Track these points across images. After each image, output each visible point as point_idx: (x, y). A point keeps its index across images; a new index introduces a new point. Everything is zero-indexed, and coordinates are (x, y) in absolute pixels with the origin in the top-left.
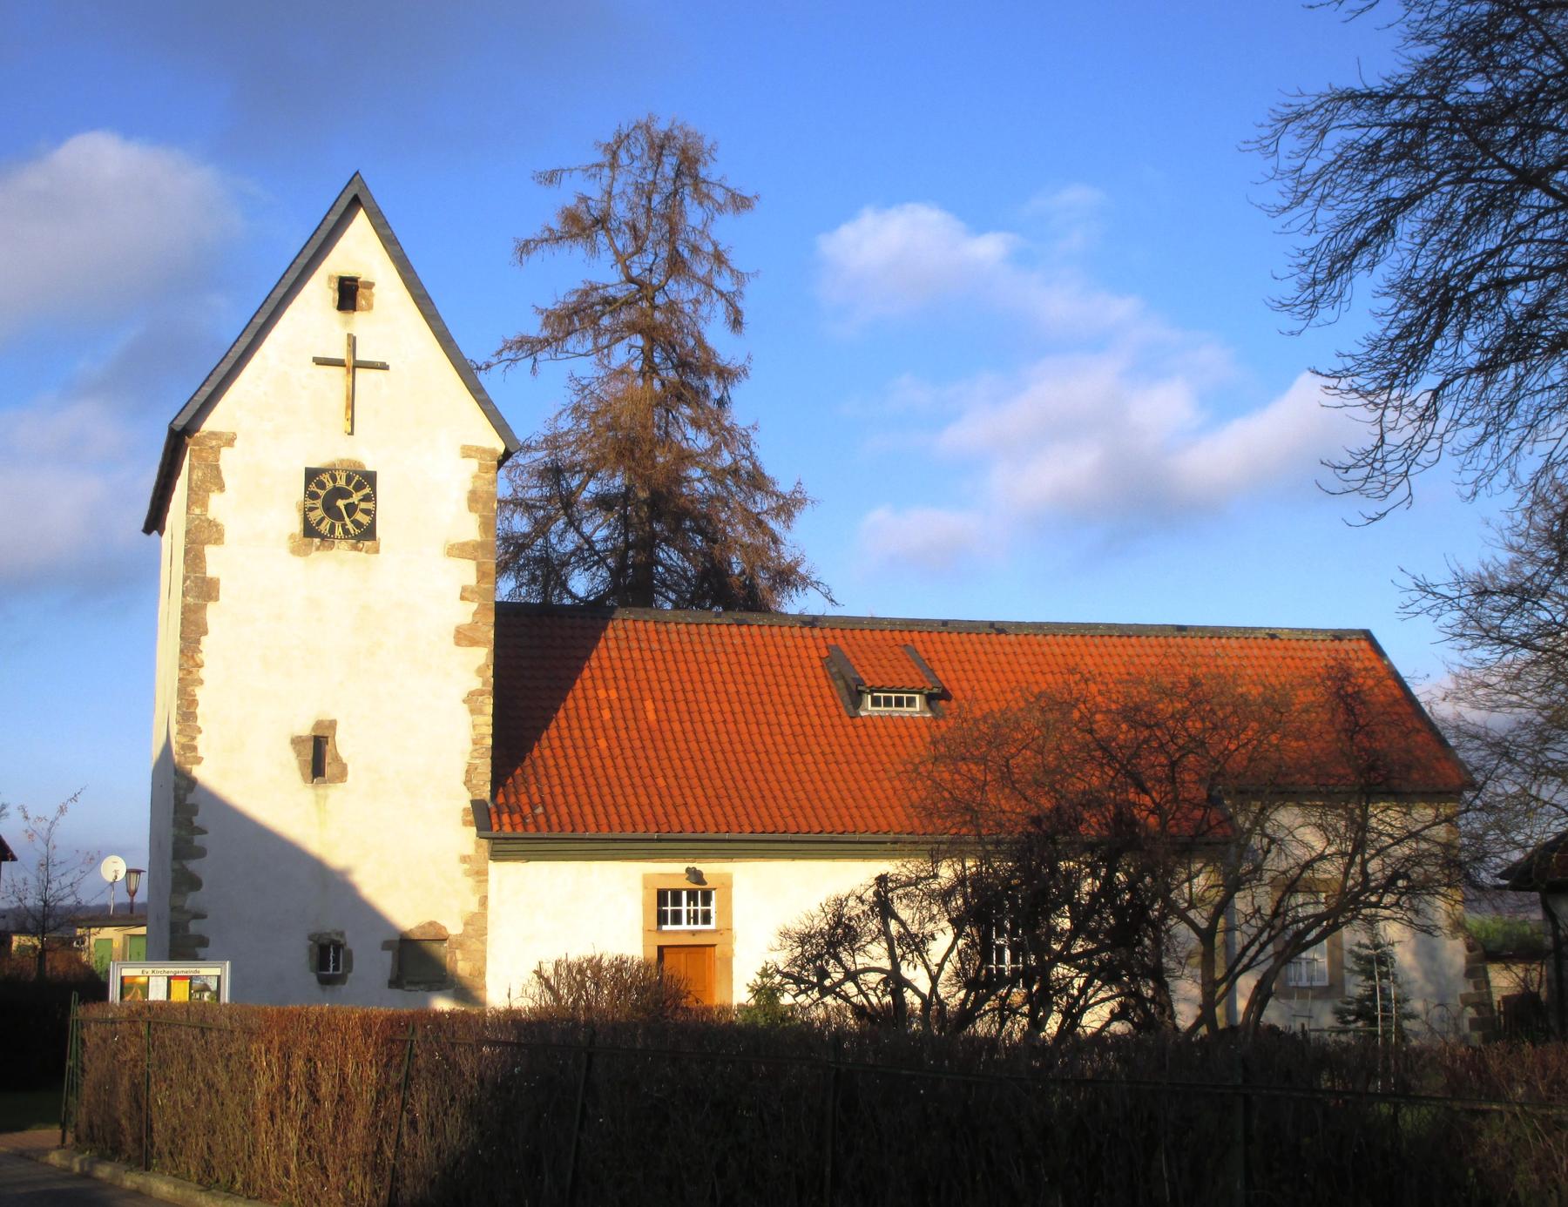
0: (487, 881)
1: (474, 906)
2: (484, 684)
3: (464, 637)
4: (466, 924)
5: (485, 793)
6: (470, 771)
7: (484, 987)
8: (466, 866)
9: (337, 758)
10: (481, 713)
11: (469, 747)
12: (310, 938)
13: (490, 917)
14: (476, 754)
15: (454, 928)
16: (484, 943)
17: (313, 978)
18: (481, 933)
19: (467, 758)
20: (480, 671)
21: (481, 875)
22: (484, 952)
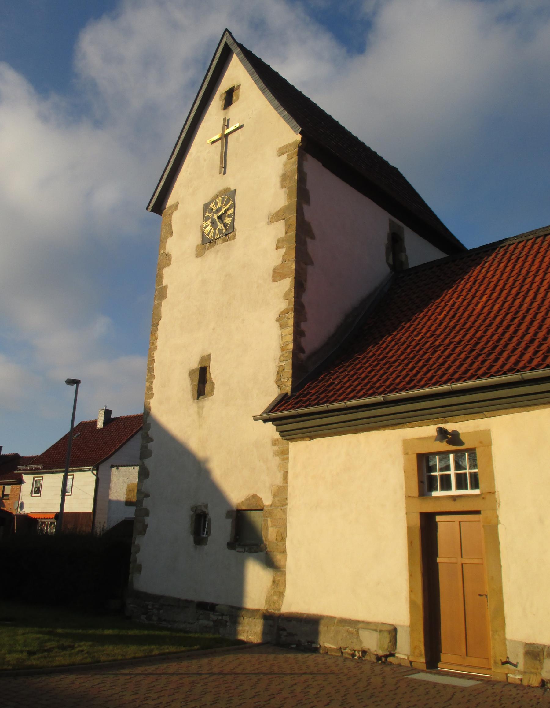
0: (288, 458)
1: (279, 481)
2: (289, 304)
3: (274, 218)
4: (274, 496)
5: (288, 388)
6: (280, 371)
7: (284, 552)
8: (276, 448)
9: (211, 379)
10: (286, 326)
11: (278, 353)
12: (192, 509)
13: (289, 489)
14: (282, 358)
15: (267, 500)
16: (284, 512)
17: (191, 538)
18: (283, 503)
19: (277, 363)
20: (286, 296)
21: (284, 454)
22: (285, 520)
